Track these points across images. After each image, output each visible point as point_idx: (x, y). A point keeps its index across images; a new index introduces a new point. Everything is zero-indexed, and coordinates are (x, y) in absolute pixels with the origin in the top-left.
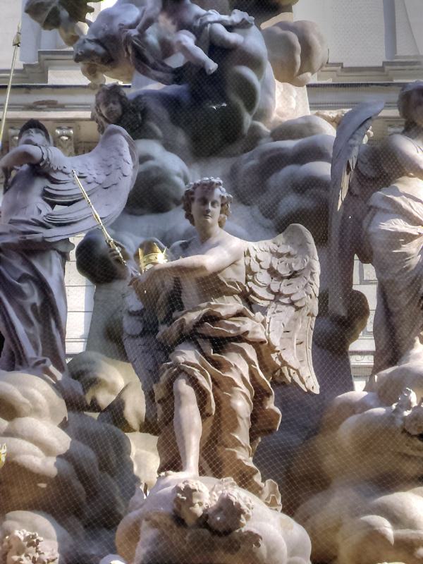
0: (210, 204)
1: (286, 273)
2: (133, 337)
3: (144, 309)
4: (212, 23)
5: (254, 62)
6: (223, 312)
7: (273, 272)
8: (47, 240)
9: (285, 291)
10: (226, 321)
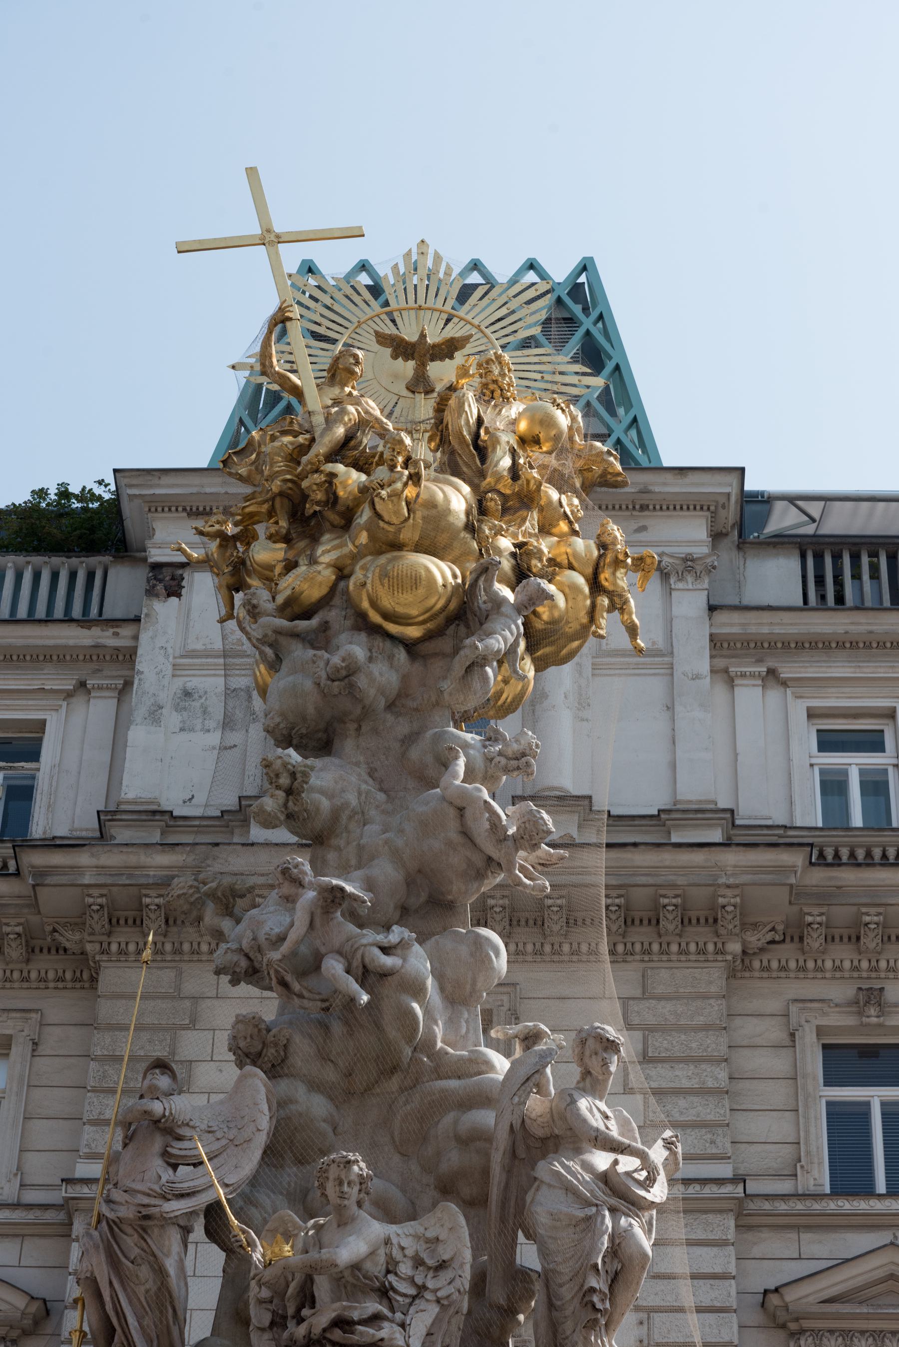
0: (346, 1185)
1: (430, 1262)
2: (262, 1330)
3: (272, 1297)
4: (365, 946)
5: (417, 990)
6: (356, 1315)
7: (418, 1262)
8: (165, 1215)
9: (430, 1284)
10: (360, 1327)
